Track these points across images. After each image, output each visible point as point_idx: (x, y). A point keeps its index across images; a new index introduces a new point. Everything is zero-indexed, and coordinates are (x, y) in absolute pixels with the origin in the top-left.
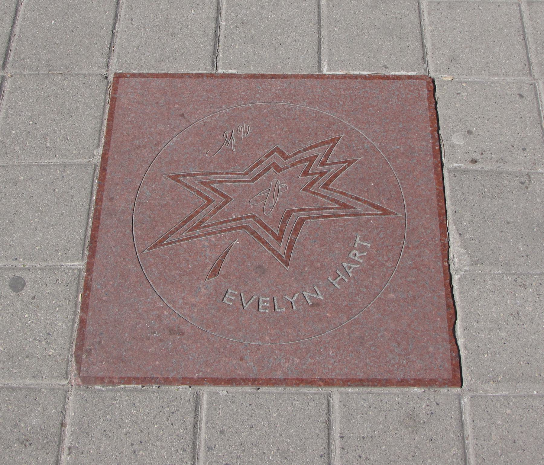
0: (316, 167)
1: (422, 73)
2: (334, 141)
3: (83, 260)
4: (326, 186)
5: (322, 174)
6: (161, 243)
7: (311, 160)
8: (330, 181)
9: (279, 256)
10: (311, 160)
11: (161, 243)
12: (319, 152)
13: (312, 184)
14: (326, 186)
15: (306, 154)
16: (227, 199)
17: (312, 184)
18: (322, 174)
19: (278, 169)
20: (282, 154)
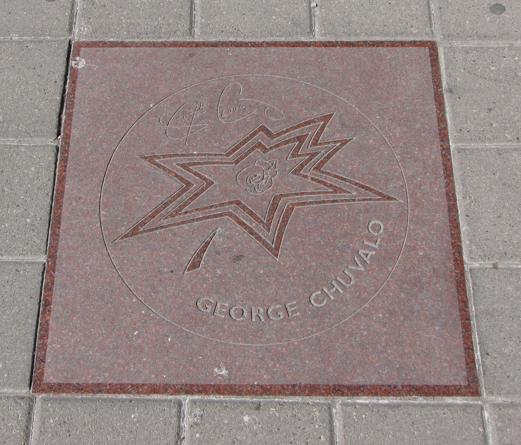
0: (307, 148)
4: (318, 168)
6: (134, 232)
7: (300, 139)
8: (323, 162)
10: (300, 139)
11: (134, 232)
13: (302, 166)
14: (318, 168)
15: (297, 132)
16: (211, 183)
17: (302, 166)
18: (313, 155)
19: (265, 150)
20: (268, 133)
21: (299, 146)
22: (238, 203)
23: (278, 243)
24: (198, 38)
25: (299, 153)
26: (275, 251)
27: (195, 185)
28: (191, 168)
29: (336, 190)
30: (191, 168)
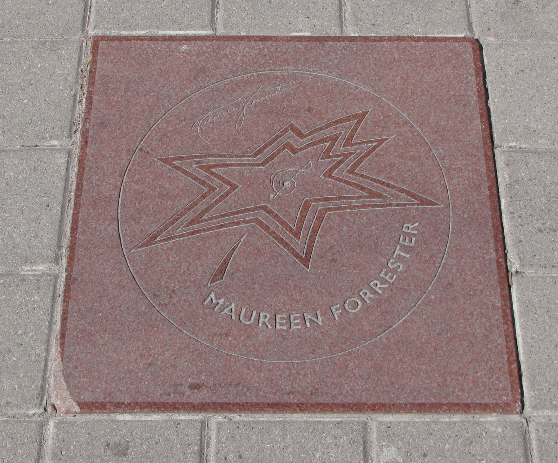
0: (339, 147)
1: (469, 35)
2: (360, 117)
3: (57, 260)
4: (351, 171)
5: (346, 156)
7: (334, 139)
9: (297, 256)
10: (334, 139)
12: (343, 131)
15: (328, 132)
18: (346, 156)
19: (294, 151)
21: (330, 147)
22: (264, 208)
23: (309, 253)
24: (221, 31)
25: (331, 154)
26: (306, 261)
27: (218, 189)
28: (213, 170)
29: (373, 194)
30: (213, 170)
